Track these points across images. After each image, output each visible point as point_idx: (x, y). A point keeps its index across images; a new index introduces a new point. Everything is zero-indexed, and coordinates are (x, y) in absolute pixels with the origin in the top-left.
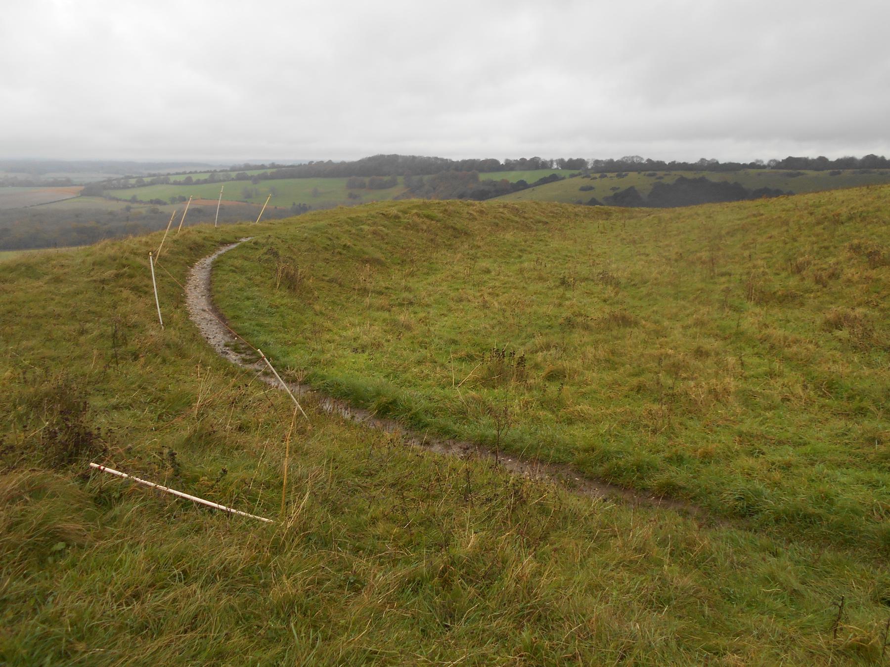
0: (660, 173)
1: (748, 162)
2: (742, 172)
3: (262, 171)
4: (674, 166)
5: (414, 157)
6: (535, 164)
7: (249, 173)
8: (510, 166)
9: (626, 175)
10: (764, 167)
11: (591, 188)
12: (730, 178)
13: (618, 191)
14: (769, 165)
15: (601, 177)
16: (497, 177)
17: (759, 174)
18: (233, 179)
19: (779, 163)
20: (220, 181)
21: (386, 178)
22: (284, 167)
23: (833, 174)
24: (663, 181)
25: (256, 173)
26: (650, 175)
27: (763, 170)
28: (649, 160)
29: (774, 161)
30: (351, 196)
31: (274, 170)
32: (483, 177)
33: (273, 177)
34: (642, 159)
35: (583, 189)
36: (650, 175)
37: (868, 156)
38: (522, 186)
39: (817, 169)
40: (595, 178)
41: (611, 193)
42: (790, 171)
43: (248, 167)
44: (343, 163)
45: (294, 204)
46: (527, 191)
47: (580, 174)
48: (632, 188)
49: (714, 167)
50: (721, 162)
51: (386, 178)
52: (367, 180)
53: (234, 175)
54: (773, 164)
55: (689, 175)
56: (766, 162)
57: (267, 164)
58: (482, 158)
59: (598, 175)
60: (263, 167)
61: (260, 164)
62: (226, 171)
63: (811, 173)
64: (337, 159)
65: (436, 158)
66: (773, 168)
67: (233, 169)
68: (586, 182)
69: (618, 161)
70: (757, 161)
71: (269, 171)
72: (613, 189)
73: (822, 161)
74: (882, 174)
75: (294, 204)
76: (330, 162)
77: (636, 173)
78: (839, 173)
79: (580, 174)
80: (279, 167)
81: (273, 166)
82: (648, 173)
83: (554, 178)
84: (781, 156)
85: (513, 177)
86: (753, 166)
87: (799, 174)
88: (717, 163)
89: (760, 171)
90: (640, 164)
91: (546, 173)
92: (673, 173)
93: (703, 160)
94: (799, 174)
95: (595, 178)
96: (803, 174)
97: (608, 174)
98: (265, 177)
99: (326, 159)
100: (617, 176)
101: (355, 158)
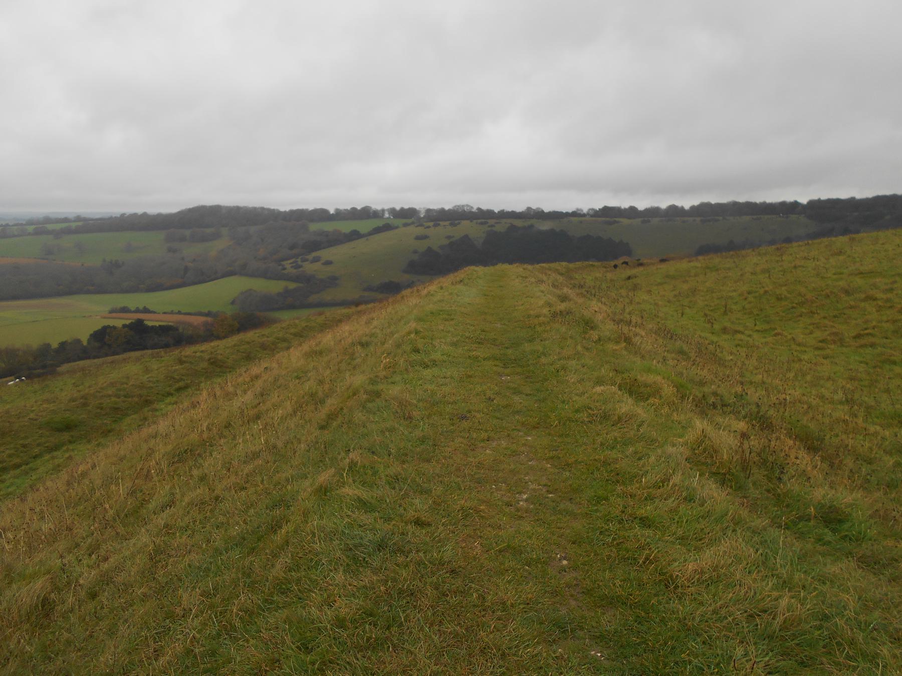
1: (570, 211)
3: (64, 225)
4: (503, 215)
5: (238, 209)
6: (366, 213)
7: (50, 227)
8: (341, 215)
10: (584, 215)
14: (588, 214)
15: (436, 225)
16: (328, 227)
17: (581, 222)
18: (29, 234)
20: (15, 236)
21: (209, 231)
22: (92, 220)
24: (494, 229)
25: (58, 226)
26: (482, 223)
27: (583, 219)
28: (479, 209)
29: (593, 209)
30: (170, 250)
31: (80, 224)
32: (314, 227)
33: (77, 231)
35: (418, 238)
36: (482, 223)
38: (355, 235)
39: (629, 218)
40: (428, 227)
41: (446, 242)
43: (48, 220)
44: (159, 215)
45: (104, 261)
46: (360, 241)
47: (413, 223)
48: (466, 236)
49: (540, 215)
50: (546, 210)
51: (209, 231)
52: (187, 233)
53: (31, 229)
54: (591, 212)
55: (519, 223)
56: (585, 211)
57: (71, 216)
59: (431, 224)
60: (66, 220)
61: (63, 216)
62: (22, 224)
63: (625, 221)
64: (153, 211)
65: (263, 209)
66: (592, 216)
67: (30, 222)
68: (420, 231)
69: (449, 210)
71: (74, 225)
72: (449, 237)
73: (633, 209)
75: (104, 261)
76: (145, 214)
77: (468, 222)
80: (85, 220)
81: (78, 219)
82: (479, 221)
83: (387, 227)
84: (598, 206)
85: (346, 227)
86: (575, 214)
88: (543, 211)
89: (581, 219)
91: (378, 223)
92: (504, 221)
93: (529, 209)
95: (428, 227)
97: (441, 223)
98: (68, 231)
99: (140, 211)
101: (174, 210)
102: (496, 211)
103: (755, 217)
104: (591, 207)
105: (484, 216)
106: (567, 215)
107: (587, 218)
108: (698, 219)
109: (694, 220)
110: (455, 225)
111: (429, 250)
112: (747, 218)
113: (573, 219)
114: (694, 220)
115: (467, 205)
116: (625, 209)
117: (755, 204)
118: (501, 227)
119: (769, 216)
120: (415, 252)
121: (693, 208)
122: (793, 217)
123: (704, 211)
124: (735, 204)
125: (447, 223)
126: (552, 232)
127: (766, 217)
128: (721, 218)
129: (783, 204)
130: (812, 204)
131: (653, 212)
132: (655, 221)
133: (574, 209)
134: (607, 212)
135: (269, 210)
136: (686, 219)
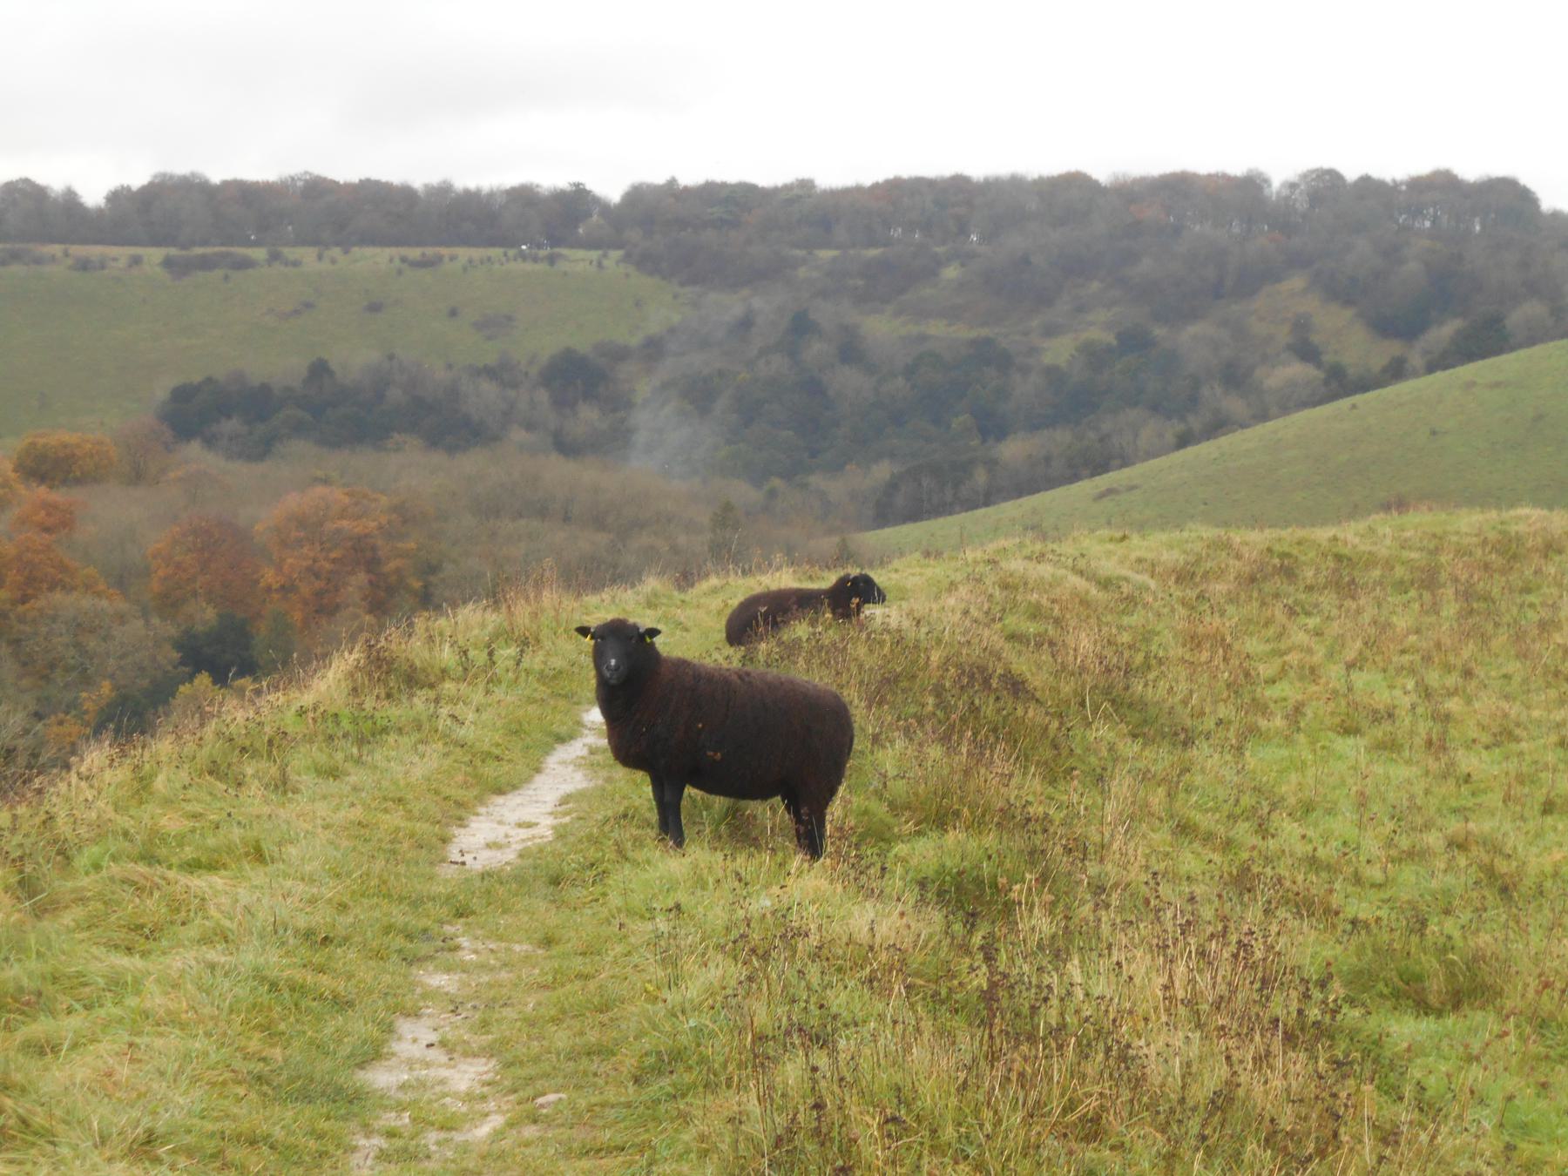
74: (84, 265)
103: (415, 253)
108: (154, 255)
109: (136, 261)
112: (379, 258)
114: (136, 261)
119: (477, 253)
121: (118, 197)
122: (578, 260)
123: (187, 224)
124: (316, 189)
127: (464, 253)
128: (259, 254)
129: (524, 197)
130: (638, 196)
135: (649, 186)
136: (95, 251)
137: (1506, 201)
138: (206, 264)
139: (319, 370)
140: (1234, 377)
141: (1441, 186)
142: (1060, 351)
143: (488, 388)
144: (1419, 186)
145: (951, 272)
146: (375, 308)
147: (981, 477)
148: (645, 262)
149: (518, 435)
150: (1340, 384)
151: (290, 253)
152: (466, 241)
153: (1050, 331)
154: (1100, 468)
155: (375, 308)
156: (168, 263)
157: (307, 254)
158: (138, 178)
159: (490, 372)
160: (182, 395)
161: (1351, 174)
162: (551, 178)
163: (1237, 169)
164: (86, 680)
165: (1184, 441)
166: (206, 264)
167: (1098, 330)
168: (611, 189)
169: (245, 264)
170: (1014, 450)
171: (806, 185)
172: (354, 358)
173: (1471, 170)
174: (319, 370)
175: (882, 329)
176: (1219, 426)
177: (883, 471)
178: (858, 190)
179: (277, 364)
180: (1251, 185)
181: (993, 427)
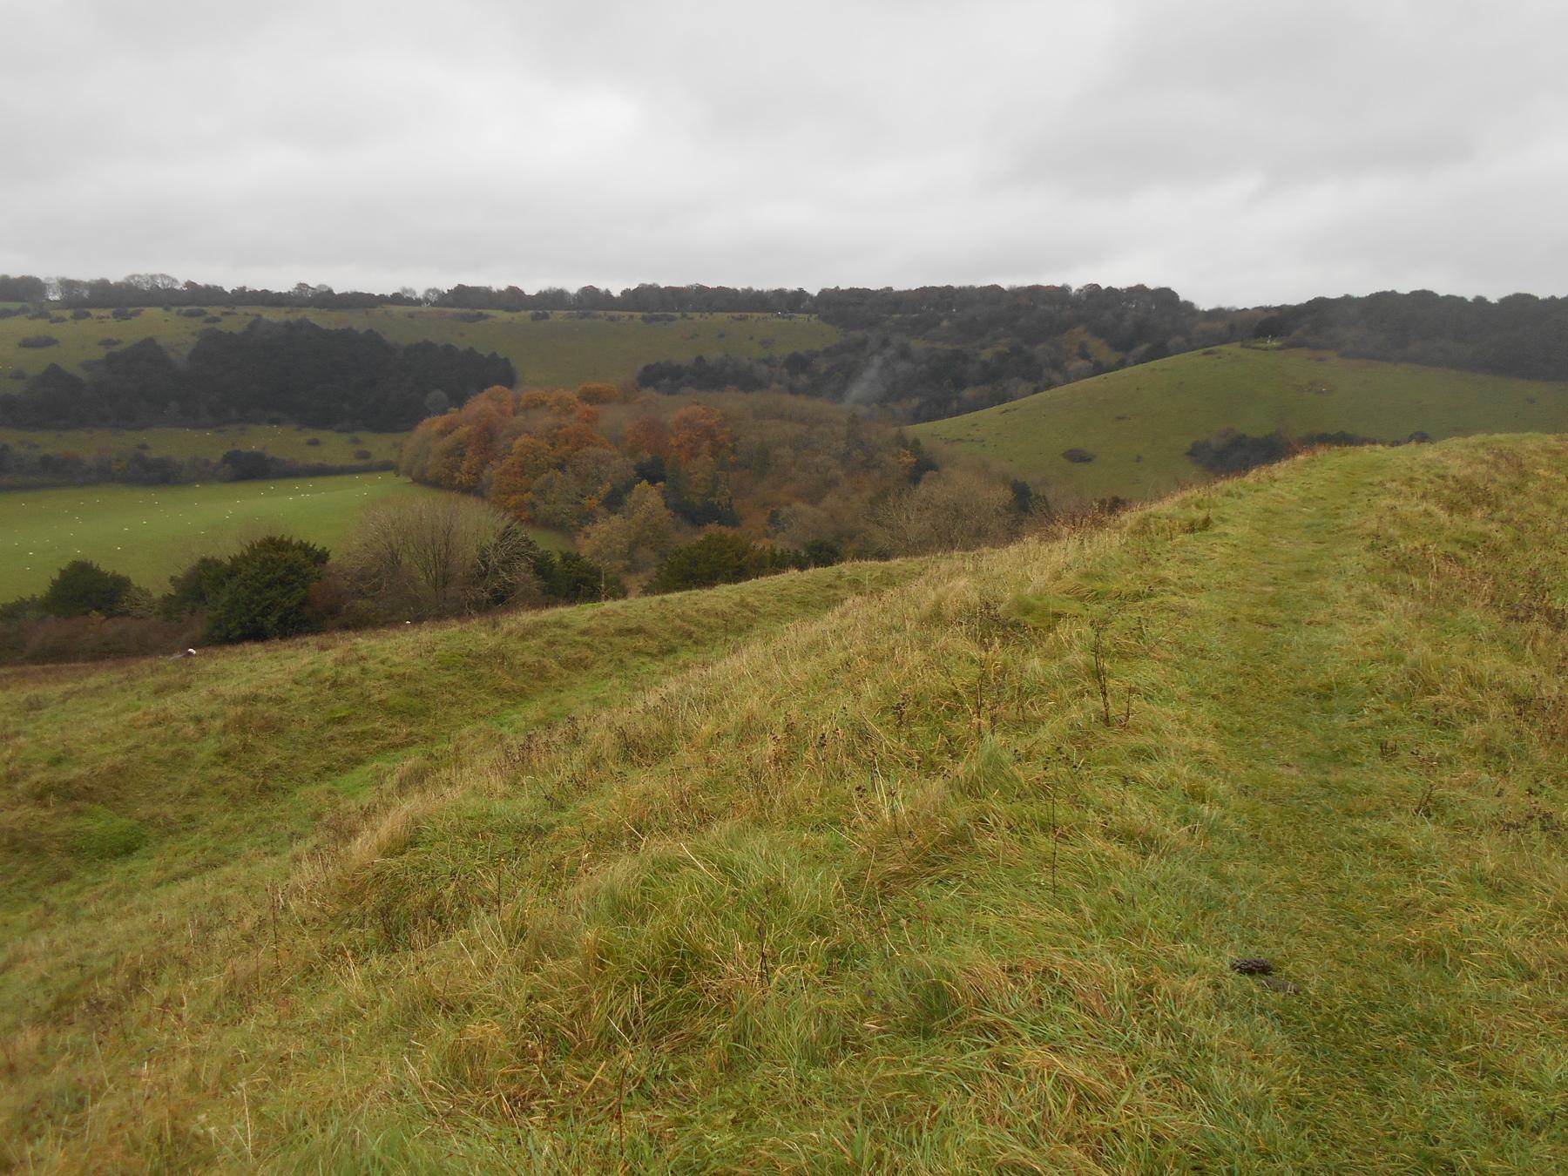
0: (212, 311)
1: (389, 293)
2: (378, 311)
4: (244, 297)
9: (137, 314)
10: (418, 302)
11: (49, 342)
12: (358, 322)
13: (117, 349)
14: (427, 300)
15: (76, 317)
17: (411, 316)
19: (442, 296)
23: (536, 318)
24: (219, 326)
26: (190, 314)
27: (417, 309)
28: (190, 284)
29: (435, 291)
34: (175, 281)
35: (27, 344)
36: (190, 314)
37: (1517, 296)
39: (508, 309)
40: (61, 320)
41: (100, 353)
42: (464, 311)
47: (24, 310)
48: (150, 342)
49: (326, 300)
50: (338, 290)
54: (433, 297)
55: (313, 316)
56: (420, 294)
58: (425, 278)
59: (68, 313)
63: (501, 315)
66: (434, 304)
68: (39, 327)
69: (118, 286)
70: (405, 290)
72: (107, 343)
73: (514, 292)
74: (612, 319)
77: (160, 310)
78: (546, 316)
79: (24, 310)
82: (184, 309)
84: (446, 284)
86: (397, 299)
87: (480, 316)
88: (330, 292)
89: (411, 309)
90: (172, 291)
92: (240, 310)
93: (1553, 297)
94: (480, 316)
95: (61, 320)
96: (486, 317)
97: (93, 311)
100: (117, 315)
102: (228, 289)
103: (736, 315)
104: (432, 286)
105: (200, 298)
106: (382, 300)
107: (425, 308)
108: (638, 315)
109: (631, 317)
110: (128, 317)
111: (54, 370)
113: (396, 309)
114: (631, 317)
115: (162, 276)
116: (500, 292)
117: (735, 291)
118: (233, 324)
119: (761, 315)
120: (18, 376)
122: (801, 318)
124: (701, 290)
125: (107, 312)
126: (347, 335)
127: (756, 315)
128: (678, 315)
129: (780, 293)
130: (824, 293)
131: (552, 300)
132: (558, 316)
133: (396, 290)
134: (463, 296)
137: (1166, 297)
138: (657, 318)
139: (700, 359)
140: (1057, 366)
141: (1140, 290)
142: (987, 355)
143: (764, 368)
144: (1130, 290)
145: (945, 323)
146: (721, 336)
147: (955, 404)
148: (826, 319)
149: (776, 386)
150: (1099, 369)
151: (689, 314)
152: (757, 311)
153: (983, 347)
154: (1003, 401)
155: (721, 336)
156: (643, 318)
157: (697, 315)
158: (633, 287)
159: (766, 362)
160: (647, 369)
161: (1104, 286)
162: (791, 286)
163: (1058, 284)
164: (600, 482)
165: (1036, 391)
166: (657, 318)
167: (1002, 346)
168: (814, 291)
169: (672, 319)
170: (968, 393)
171: (889, 289)
172: (713, 355)
173: (1152, 284)
174: (700, 359)
175: (917, 345)
176: (1050, 385)
177: (916, 401)
178: (910, 291)
179: (684, 358)
180: (1064, 290)
181: (960, 384)
